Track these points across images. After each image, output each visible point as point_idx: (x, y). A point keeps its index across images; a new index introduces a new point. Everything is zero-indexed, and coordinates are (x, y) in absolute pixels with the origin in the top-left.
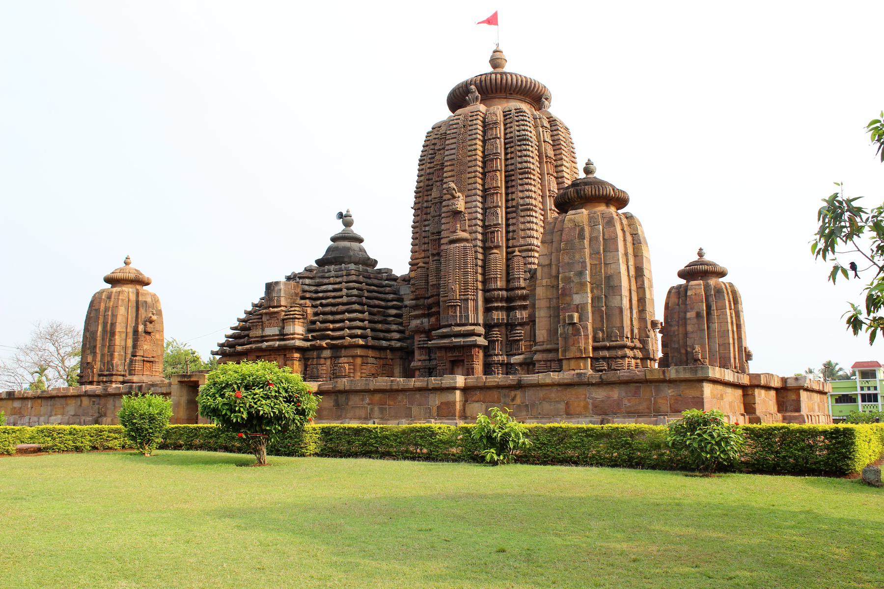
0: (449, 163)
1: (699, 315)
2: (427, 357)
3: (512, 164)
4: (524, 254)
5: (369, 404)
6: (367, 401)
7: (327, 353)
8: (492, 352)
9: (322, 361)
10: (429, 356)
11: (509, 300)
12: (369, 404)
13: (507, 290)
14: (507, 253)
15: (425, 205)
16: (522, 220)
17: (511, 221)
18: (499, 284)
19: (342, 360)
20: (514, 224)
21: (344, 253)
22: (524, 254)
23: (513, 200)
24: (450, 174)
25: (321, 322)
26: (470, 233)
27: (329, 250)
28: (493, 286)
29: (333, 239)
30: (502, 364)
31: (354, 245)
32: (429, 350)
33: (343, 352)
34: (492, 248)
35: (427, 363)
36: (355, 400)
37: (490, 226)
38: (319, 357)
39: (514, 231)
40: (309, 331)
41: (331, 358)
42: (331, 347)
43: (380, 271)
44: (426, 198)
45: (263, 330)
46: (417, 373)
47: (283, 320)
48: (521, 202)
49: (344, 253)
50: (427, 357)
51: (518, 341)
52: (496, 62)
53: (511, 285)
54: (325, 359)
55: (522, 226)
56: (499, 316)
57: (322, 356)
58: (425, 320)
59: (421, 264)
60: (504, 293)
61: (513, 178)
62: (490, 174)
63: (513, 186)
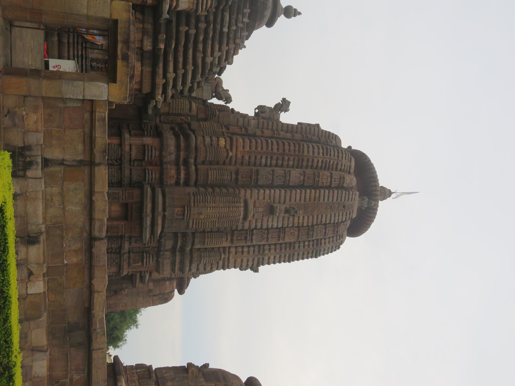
0: (317, 195)
1: (150, 291)
2: (133, 156)
3: (299, 247)
5: (71, 380)
6: (76, 377)
7: (148, 46)
8: (133, 240)
10: (135, 160)
11: (182, 250)
12: (71, 380)
13: (191, 250)
14: (224, 248)
15: (286, 158)
16: (251, 259)
18: (197, 246)
20: (248, 252)
23: (270, 250)
24: (308, 197)
25: (187, 32)
26: (250, 221)
28: (197, 240)
30: (120, 248)
32: (140, 186)
33: (148, 69)
34: (232, 236)
35: (127, 157)
36: (77, 357)
37: (252, 235)
38: (144, 32)
39: (243, 252)
40: (179, 14)
41: (141, 48)
44: (292, 158)
46: (115, 141)
50: (133, 156)
51: (143, 261)
53: (195, 255)
54: (142, 41)
55: (245, 260)
56: (169, 244)
57: (145, 38)
58: (173, 157)
59: (230, 154)
60: (188, 249)
61: (288, 249)
62: (296, 233)
63: (281, 250)
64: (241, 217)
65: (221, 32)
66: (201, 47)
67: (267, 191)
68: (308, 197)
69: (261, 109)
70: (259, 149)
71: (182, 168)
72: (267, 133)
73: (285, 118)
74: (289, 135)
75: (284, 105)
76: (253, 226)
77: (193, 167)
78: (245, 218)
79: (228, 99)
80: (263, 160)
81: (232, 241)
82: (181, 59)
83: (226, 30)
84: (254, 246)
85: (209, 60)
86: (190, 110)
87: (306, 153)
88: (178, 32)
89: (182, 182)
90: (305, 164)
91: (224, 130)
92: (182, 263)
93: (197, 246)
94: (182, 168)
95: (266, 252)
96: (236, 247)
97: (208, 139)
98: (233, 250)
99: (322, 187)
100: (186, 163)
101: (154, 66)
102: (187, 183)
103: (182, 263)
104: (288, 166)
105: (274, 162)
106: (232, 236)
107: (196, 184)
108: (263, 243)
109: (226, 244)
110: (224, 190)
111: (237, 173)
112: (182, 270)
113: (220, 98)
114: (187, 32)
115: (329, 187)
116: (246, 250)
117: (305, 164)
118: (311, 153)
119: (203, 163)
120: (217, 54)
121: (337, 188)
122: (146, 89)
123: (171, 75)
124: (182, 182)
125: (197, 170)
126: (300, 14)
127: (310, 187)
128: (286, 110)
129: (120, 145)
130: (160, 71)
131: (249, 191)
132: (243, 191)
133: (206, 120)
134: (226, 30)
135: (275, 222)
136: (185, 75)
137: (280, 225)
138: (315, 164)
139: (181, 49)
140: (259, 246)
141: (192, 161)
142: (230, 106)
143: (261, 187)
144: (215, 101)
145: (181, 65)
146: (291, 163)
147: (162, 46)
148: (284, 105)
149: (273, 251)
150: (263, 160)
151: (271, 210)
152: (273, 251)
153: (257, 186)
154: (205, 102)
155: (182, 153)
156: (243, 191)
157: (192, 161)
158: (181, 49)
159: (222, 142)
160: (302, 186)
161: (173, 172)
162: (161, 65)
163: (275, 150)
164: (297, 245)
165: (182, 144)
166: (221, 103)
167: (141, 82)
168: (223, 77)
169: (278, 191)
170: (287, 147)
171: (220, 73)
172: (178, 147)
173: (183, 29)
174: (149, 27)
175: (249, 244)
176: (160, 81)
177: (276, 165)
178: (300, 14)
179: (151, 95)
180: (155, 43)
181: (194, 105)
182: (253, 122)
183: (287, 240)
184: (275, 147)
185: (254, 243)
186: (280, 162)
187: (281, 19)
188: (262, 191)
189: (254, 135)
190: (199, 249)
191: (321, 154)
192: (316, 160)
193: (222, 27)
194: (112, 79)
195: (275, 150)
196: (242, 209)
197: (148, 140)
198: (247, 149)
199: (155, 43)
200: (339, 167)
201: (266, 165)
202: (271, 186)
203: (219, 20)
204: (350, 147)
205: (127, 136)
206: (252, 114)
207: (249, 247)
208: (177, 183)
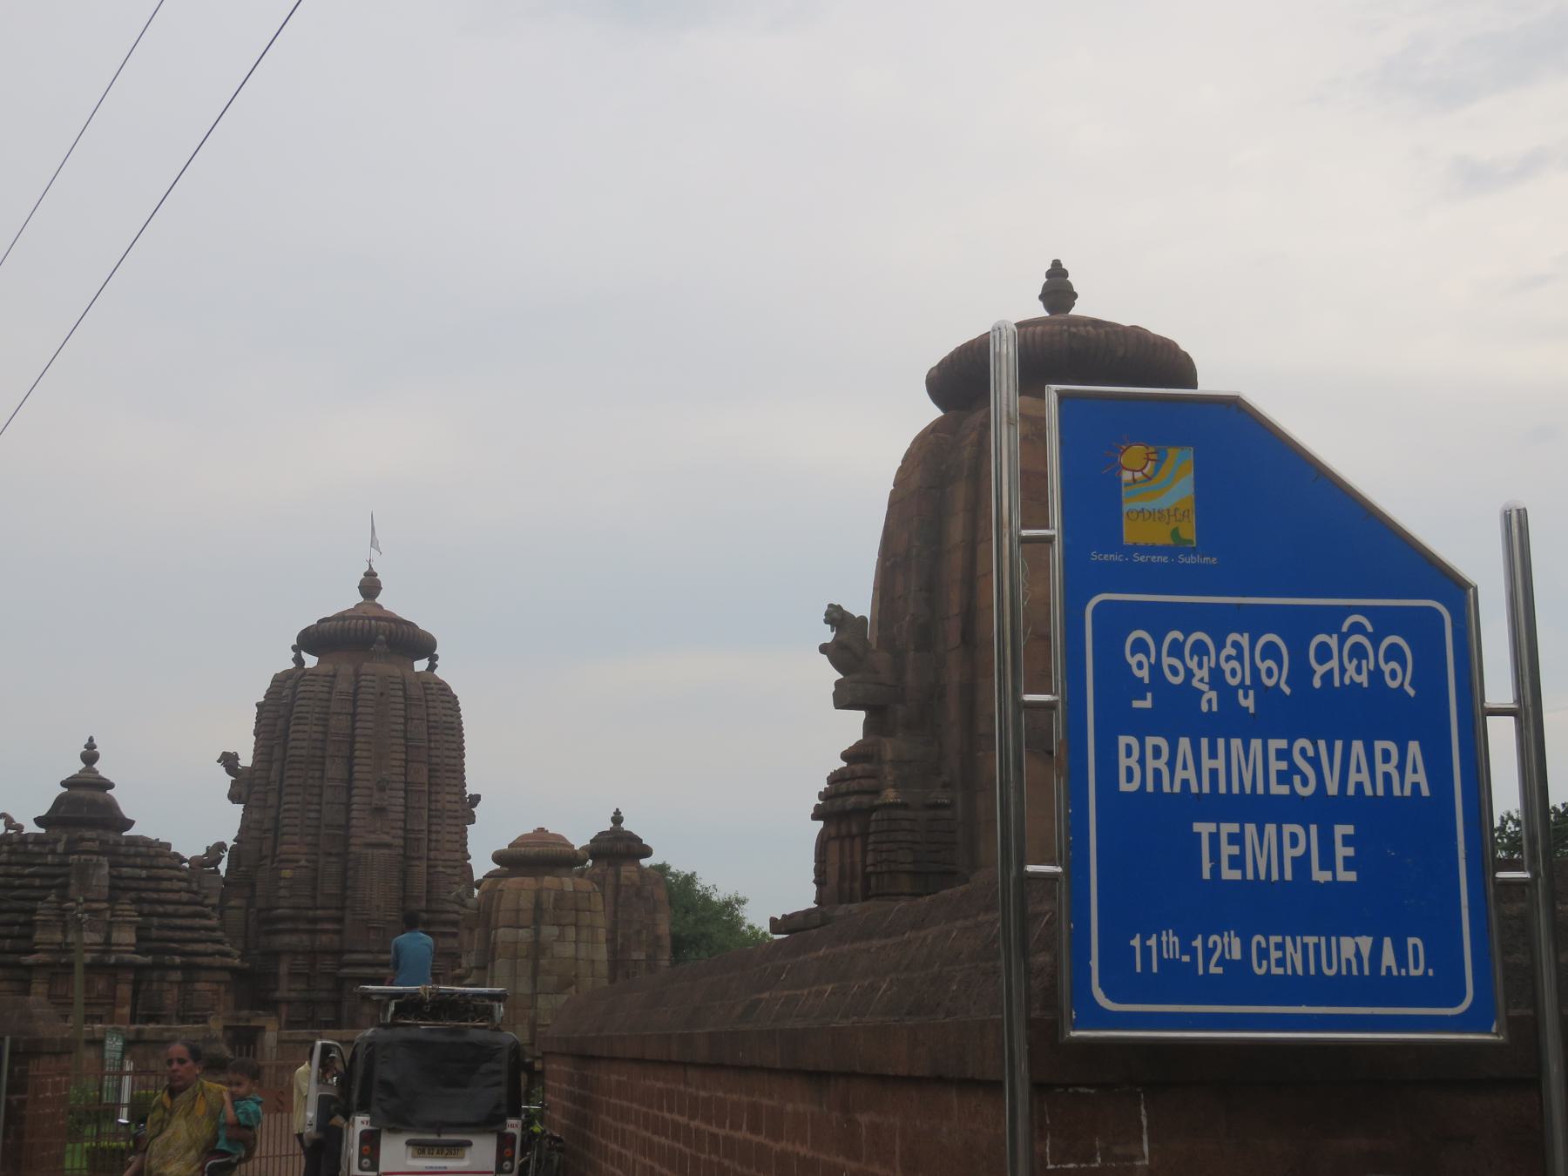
2: (303, 986)
4: (449, 871)
7: (176, 976)
9: (166, 986)
13: (427, 911)
15: (310, 782)
17: (434, 828)
19: (199, 986)
20: (438, 832)
21: (86, 805)
22: (449, 871)
24: (365, 754)
27: (60, 801)
29: (63, 784)
31: (98, 795)
34: (413, 858)
40: (139, 939)
42: (185, 967)
43: (134, 841)
45: (65, 932)
47: (111, 923)
48: (448, 806)
49: (86, 805)
50: (303, 986)
52: (370, 586)
54: (172, 983)
55: (448, 837)
58: (305, 938)
59: (303, 863)
64: (386, 851)
65: (149, 878)
66: (170, 908)
67: (355, 814)
68: (365, 754)
69: (234, 797)
70: (297, 822)
71: (319, 927)
72: (272, 799)
73: (246, 760)
74: (276, 766)
75: (229, 761)
76: (400, 832)
77: (320, 913)
78: (388, 846)
79: (221, 846)
80: (312, 815)
81: (419, 858)
82: (189, 935)
83: (144, 873)
84: (429, 825)
85: (185, 897)
86: (239, 908)
87: (303, 752)
88: (158, 940)
89: (336, 927)
90: (319, 753)
91: (268, 861)
92: (445, 923)
93: (424, 904)
94: (319, 927)
95: (439, 806)
96: (429, 850)
97: (283, 892)
98: (432, 854)
99: (354, 729)
100: (315, 920)
101: (200, 967)
102: (340, 920)
103: (445, 923)
104: (322, 778)
105: (315, 800)
106: (413, 858)
107: (342, 908)
108: (425, 813)
109: (424, 864)
110: (350, 873)
111: (330, 854)
112: (455, 924)
113: (219, 860)
114: (161, 927)
115: (354, 715)
116: (434, 837)
117: (319, 753)
118: (305, 744)
119: (314, 898)
120: (177, 885)
121: (354, 702)
122: (225, 976)
123: (211, 947)
124: (336, 927)
125: (323, 908)
126: (91, 740)
127: (352, 750)
128: (235, 757)
129: (289, 1002)
130: (205, 960)
131: (352, 841)
132: (353, 849)
133: (253, 886)
134: (144, 873)
135: (396, 800)
136: (207, 929)
137: (402, 794)
138: (320, 736)
139: (178, 934)
140: (430, 817)
141: (311, 913)
142: (230, 843)
143: (349, 819)
144: (223, 867)
145: (196, 935)
146: (318, 774)
147: (178, 960)
148: (229, 761)
149: (439, 797)
150: (312, 815)
151: (380, 811)
152: (439, 797)
153: (347, 826)
154: (225, 881)
155: (302, 926)
156: (353, 849)
157: (311, 913)
158: (178, 934)
159: (287, 873)
160: (350, 760)
161: (325, 939)
162: (199, 960)
163: (299, 798)
164: (434, 760)
165: (289, 925)
166: (226, 854)
167: (218, 982)
168: (187, 854)
169: (355, 799)
170: (295, 781)
171: (183, 860)
172: (294, 931)
173: (154, 933)
174: (155, 975)
175: (424, 835)
176: (218, 961)
177: (320, 795)
178: (91, 740)
179: (233, 970)
180: (174, 967)
181: (232, 903)
182: (256, 816)
183: (425, 780)
184: (294, 798)
185: (424, 827)
186: (316, 791)
187: (103, 768)
188: (354, 822)
189: (276, 819)
190: (428, 901)
191: (306, 728)
192: (315, 736)
193: (140, 879)
194: (262, 1029)
195: (299, 798)
196: (376, 852)
197: (283, 969)
198: (296, 838)
199: (174, 967)
200: (325, 696)
201: (319, 811)
202: (348, 806)
203: (134, 884)
204: (294, 648)
205: (278, 995)
206: (239, 809)
207: (430, 832)
208: (338, 932)
